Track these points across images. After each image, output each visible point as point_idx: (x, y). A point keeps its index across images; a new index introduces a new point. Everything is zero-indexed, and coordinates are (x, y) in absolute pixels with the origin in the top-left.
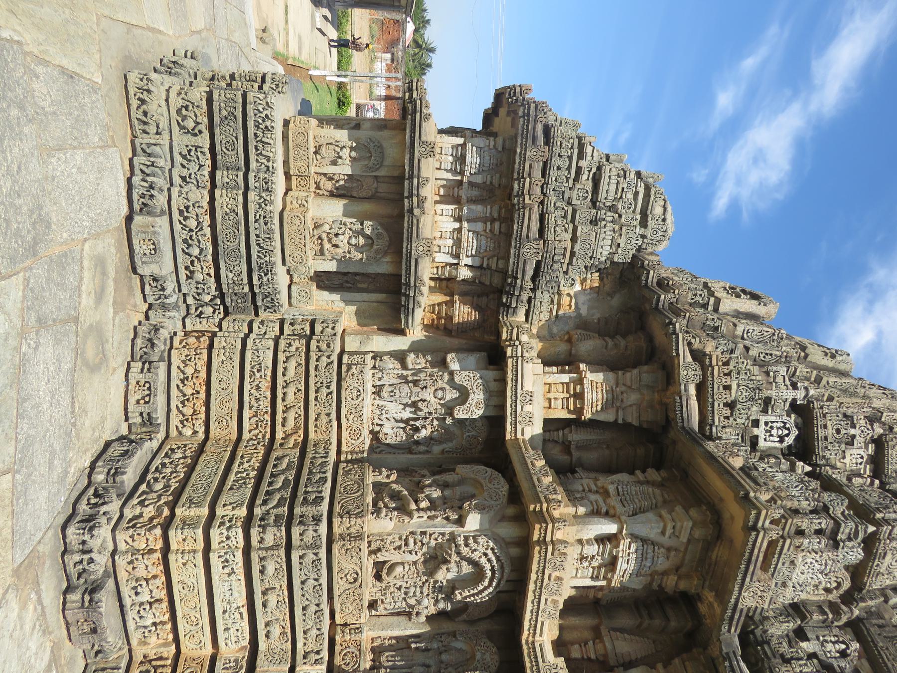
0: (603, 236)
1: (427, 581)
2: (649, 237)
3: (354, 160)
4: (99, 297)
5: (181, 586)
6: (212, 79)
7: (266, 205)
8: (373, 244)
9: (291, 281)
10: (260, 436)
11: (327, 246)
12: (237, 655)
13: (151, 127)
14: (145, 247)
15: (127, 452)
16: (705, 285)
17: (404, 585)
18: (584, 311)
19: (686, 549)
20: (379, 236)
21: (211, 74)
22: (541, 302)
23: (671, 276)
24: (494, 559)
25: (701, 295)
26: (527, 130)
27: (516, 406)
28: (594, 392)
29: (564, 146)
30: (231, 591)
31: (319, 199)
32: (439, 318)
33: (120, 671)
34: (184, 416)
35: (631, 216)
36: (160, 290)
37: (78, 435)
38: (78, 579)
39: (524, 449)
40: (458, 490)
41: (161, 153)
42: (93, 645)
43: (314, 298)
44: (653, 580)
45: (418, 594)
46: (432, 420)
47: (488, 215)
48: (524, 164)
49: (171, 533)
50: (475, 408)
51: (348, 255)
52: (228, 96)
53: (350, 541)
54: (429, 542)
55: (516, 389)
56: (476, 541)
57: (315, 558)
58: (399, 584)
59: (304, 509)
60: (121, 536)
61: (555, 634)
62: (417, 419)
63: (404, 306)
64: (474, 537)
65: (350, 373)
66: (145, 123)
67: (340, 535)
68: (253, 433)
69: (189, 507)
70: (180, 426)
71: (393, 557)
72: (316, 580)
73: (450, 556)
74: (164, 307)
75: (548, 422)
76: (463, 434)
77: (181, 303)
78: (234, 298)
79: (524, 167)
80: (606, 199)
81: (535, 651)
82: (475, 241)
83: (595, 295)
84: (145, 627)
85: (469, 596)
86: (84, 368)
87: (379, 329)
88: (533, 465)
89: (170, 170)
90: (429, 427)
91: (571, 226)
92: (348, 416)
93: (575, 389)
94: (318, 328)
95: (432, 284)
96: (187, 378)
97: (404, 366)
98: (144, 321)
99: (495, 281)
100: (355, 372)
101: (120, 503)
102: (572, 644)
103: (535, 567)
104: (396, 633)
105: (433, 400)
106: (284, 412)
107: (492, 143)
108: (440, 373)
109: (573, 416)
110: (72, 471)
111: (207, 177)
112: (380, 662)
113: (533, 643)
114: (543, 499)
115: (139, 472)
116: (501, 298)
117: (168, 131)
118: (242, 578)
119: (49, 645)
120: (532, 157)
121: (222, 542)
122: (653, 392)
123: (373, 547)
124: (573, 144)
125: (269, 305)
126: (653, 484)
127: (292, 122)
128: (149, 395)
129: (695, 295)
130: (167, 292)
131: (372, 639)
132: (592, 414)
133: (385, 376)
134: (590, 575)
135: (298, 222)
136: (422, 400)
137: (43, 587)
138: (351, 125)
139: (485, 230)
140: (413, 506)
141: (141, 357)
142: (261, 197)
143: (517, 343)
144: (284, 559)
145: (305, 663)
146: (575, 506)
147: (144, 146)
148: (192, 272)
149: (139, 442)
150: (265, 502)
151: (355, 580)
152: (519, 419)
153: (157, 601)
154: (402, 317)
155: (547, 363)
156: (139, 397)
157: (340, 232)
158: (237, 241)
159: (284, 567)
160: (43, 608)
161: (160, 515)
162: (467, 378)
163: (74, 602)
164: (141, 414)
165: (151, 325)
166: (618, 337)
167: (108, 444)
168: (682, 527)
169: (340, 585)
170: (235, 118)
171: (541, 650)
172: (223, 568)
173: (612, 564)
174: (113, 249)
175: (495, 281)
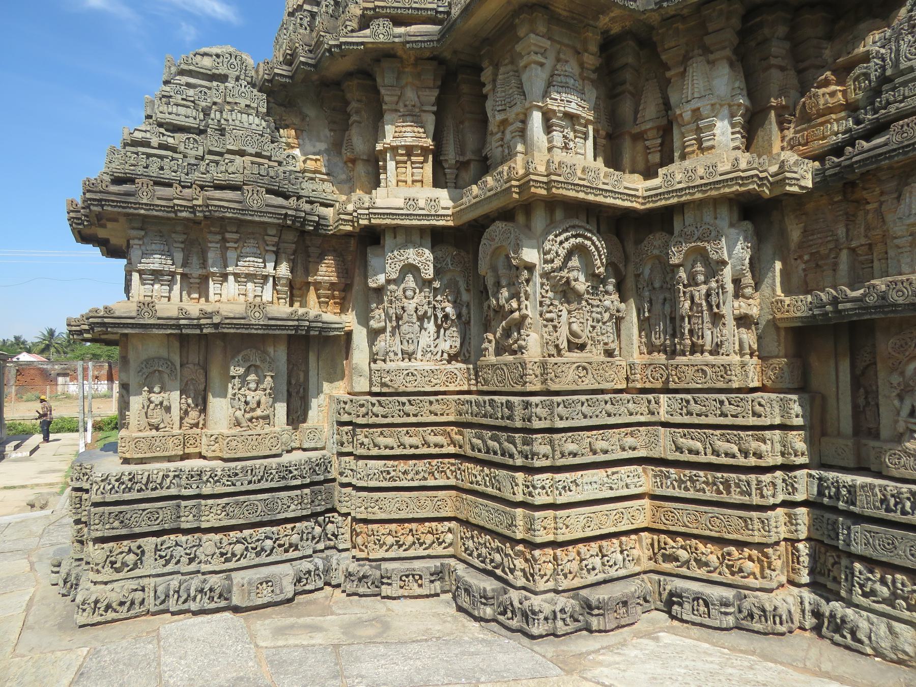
0: (237, 123)
1: (587, 301)
2: (237, 73)
3: (163, 389)
4: (315, 628)
5: (587, 529)
6: (81, 542)
7: (216, 475)
8: (256, 367)
9: (298, 449)
10: (453, 468)
11: (259, 412)
12: (650, 475)
13: (136, 597)
14: (265, 592)
15: (466, 590)
16: (291, 14)
17: (590, 323)
18: (322, 146)
19: (559, 43)
20: (245, 359)
21: (76, 544)
22: (313, 191)
23: (282, 51)
24: (565, 235)
25: (301, 19)
26: (117, 202)
27: (419, 215)
28: (405, 134)
29: (134, 162)
30: (592, 483)
31: (209, 423)
32: (334, 297)
33: (662, 579)
34: (434, 542)
35: (215, 91)
36: (310, 575)
37: (448, 635)
38: (579, 621)
39: (462, 207)
40: (502, 271)
41: (164, 585)
42: (638, 604)
43: (316, 425)
44: (589, 79)
45: (599, 310)
46: (437, 301)
47: (218, 245)
48: (158, 206)
49: (538, 540)
50: (423, 258)
51: (268, 391)
52: (97, 522)
54: (550, 298)
55: (402, 215)
56: (549, 252)
57: (562, 405)
59: (517, 418)
60: (541, 585)
61: (636, 176)
62: (436, 316)
63: (320, 332)
64: (545, 254)
65: (390, 383)
66: (133, 603)
67: (542, 383)
68: (449, 475)
69: (516, 526)
70: (444, 545)
71: (564, 332)
72: (583, 404)
73: (562, 277)
74: (327, 571)
75: (436, 184)
76: (450, 270)
77: (324, 555)
78: (317, 503)
79: (161, 206)
80: (195, 119)
81: (652, 196)
82: (248, 259)
83: (305, 133)
84: (624, 560)
86: (385, 635)
87: (347, 358)
88: (477, 197)
89: (183, 574)
90: (443, 305)
91: (226, 156)
93: (402, 155)
94: (345, 418)
95: (297, 305)
96: (397, 542)
97: (383, 330)
98: (342, 588)
99: (291, 238)
100: (388, 378)
101: (512, 590)
102: (647, 161)
103: (572, 194)
104: (635, 331)
105: (415, 300)
106: (429, 446)
107: (136, 242)
108: (389, 293)
109: (431, 157)
110: (482, 636)
111: (189, 537)
113: (644, 198)
114: (508, 185)
115: (485, 577)
116: (309, 232)
117: (140, 580)
118: (580, 473)
119: (635, 641)
120: (147, 196)
121: (547, 493)
123: (554, 352)
124: (133, 153)
125: (323, 468)
126: (495, 75)
127: (124, 456)
128: (413, 576)
129: (301, 25)
130: (312, 568)
132: (427, 137)
133: (392, 349)
134: (582, 141)
135: (234, 443)
136: (416, 312)
137: (584, 650)
138: (124, 392)
139: (236, 248)
140: (516, 315)
141: (377, 587)
142: (207, 481)
143: (355, 214)
144: (563, 434)
146: (516, 154)
147: (158, 602)
148: (291, 545)
149: (458, 579)
150: (511, 456)
151: (584, 368)
152: (433, 213)
153: (601, 551)
154: (332, 334)
155: (377, 184)
156: (416, 585)
157: (243, 400)
158: (256, 502)
159: (570, 434)
160: (603, 648)
161: (523, 553)
162: (393, 266)
163: (599, 623)
164: (432, 582)
165: (345, 581)
166: (348, 109)
167: (460, 609)
168: (535, 45)
169: (589, 383)
170: (121, 512)
171: (650, 190)
172: (571, 491)
173: (571, 118)
174: (267, 622)
175: (291, 238)
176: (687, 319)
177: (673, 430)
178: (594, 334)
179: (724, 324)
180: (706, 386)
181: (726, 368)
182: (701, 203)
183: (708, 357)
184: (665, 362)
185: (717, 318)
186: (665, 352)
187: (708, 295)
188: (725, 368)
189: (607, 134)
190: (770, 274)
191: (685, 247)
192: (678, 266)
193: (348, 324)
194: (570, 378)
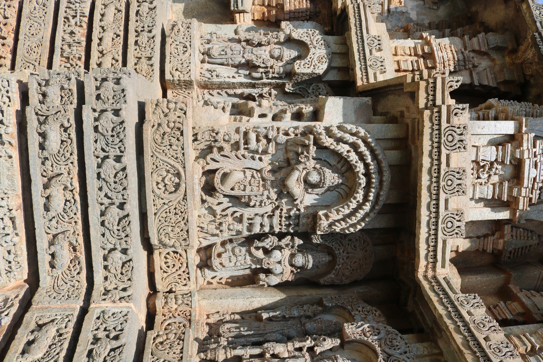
1: (277, 208)
24: (367, 153)
27: (364, 50)
32: (269, 12)
55: (362, 33)
65: (176, 29)
92: (174, 72)
93: (423, 50)
113: (435, 277)
122: (503, 57)
145: (104, 300)
151: (177, 186)
152: (368, 63)
159: (74, 136)
171: (448, 283)
176: (257, 351)
178: (230, 219)
189: (500, 252)
191: (372, 339)
193: (242, 19)
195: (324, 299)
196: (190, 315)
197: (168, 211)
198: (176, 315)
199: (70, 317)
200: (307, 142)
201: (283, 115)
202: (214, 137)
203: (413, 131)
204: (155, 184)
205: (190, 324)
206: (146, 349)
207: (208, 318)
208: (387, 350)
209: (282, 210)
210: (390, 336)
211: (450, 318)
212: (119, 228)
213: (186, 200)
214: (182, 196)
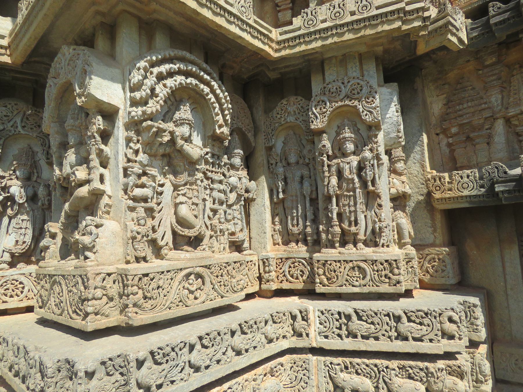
1: (204, 173)
17: (209, 204)
45: (222, 187)
53: (128, 296)
54: (141, 163)
58: (208, 212)
64: (132, 90)
67: (121, 312)
71: (166, 220)
81: (288, 40)
85: (224, 116)
112: (299, 234)
113: (279, 43)
123: (148, 252)
131: (275, 244)
140: (83, 191)
145: (307, 335)
151: (199, 276)
169: (206, 299)
176: (334, 200)
177: (329, 359)
178: (215, 221)
179: (380, 206)
180: (366, 290)
181: (391, 264)
182: (344, 56)
183: (369, 252)
184: (307, 255)
185: (371, 197)
186: (305, 242)
187: (361, 168)
188: (390, 264)
190: (417, 148)
191: (329, 108)
192: (320, 133)
194: (172, 297)
195: (267, 145)
196: (281, 259)
197: (219, 284)
198: (281, 271)
199: (328, 363)
200: (154, 129)
201: (105, 154)
202: (143, 237)
203: (134, 7)
204: (197, 301)
205: (291, 258)
206: (337, 292)
207: (278, 244)
208: (341, 97)
209: (207, 170)
210: (327, 93)
211: (326, 38)
212: (249, 332)
213: (210, 265)
214: (207, 270)
